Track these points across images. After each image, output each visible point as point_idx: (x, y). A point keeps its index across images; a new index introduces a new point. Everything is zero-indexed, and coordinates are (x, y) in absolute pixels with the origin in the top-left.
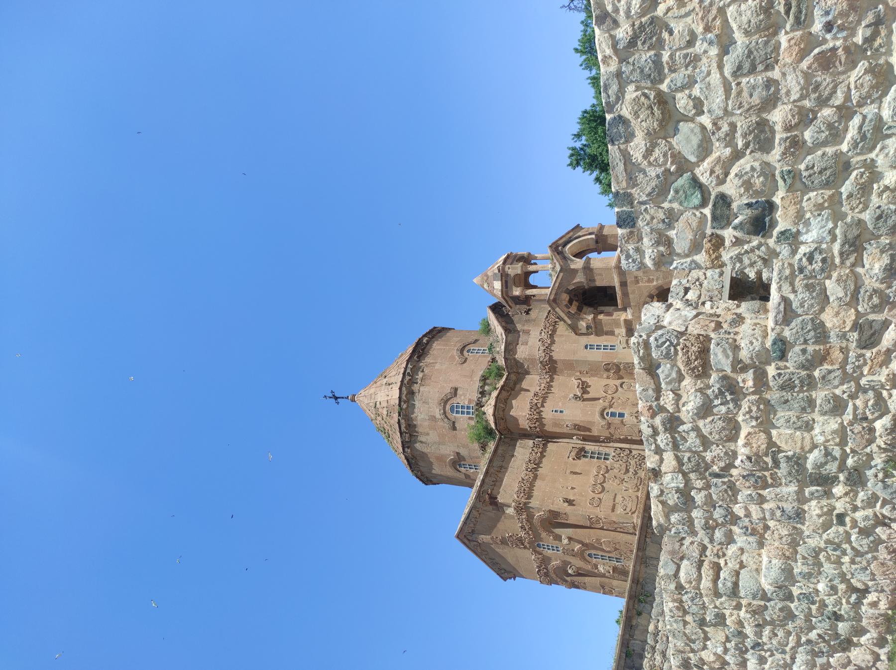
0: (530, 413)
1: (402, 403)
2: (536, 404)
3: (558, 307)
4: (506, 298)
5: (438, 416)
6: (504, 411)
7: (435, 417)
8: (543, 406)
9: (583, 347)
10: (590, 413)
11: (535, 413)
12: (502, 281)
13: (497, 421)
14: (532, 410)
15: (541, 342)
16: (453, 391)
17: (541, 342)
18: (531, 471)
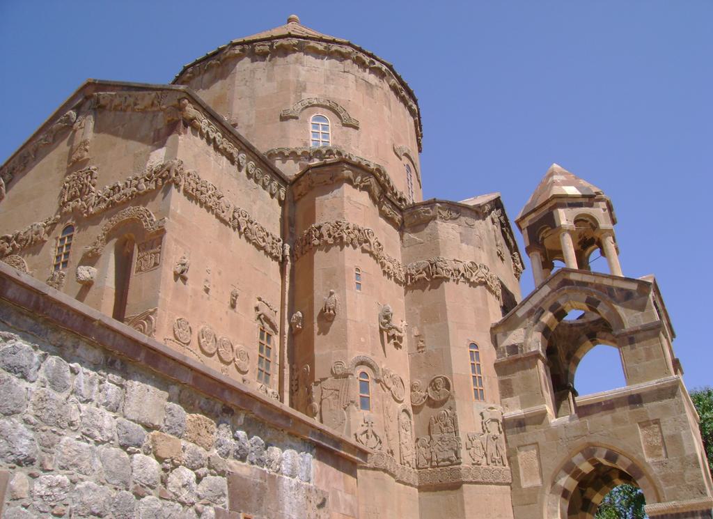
0: (351, 226)
1: (324, 44)
2: (366, 241)
3: (553, 291)
4: (549, 205)
5: (305, 96)
6: (350, 181)
7: (304, 89)
8: (364, 251)
9: (473, 340)
10: (362, 340)
11: (352, 236)
12: (583, 196)
13: (327, 169)
14: (356, 232)
15: (471, 265)
16: (354, 123)
17: (471, 265)
18: (234, 218)
